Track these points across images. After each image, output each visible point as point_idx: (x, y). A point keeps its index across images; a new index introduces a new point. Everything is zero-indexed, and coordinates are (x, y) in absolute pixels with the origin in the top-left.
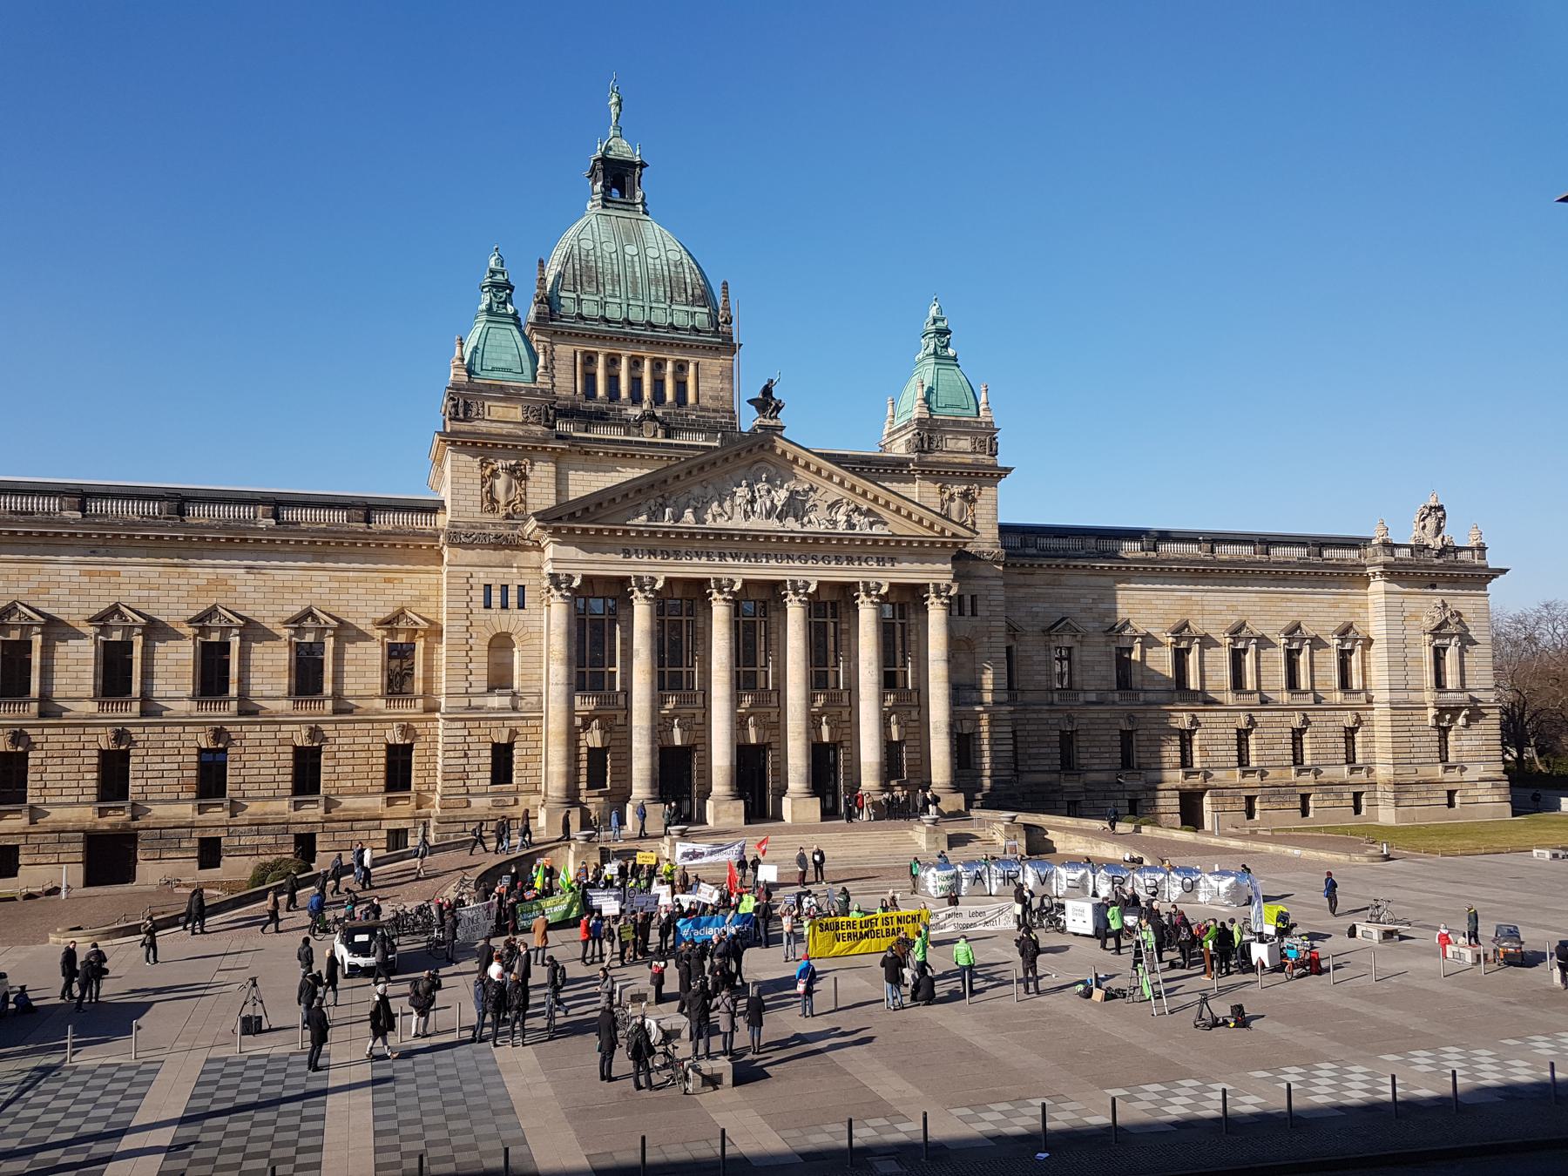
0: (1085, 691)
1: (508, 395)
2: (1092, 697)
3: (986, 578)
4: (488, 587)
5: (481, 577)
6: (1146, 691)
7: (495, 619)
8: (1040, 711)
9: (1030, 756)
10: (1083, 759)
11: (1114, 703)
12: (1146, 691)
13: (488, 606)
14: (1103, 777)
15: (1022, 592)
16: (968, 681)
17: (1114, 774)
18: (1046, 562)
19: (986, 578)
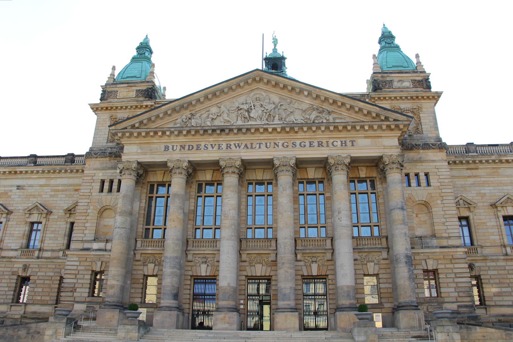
3: (434, 161)
4: (103, 182)
5: (100, 175)
8: (498, 260)
15: (471, 181)
18: (484, 159)
19: (434, 161)
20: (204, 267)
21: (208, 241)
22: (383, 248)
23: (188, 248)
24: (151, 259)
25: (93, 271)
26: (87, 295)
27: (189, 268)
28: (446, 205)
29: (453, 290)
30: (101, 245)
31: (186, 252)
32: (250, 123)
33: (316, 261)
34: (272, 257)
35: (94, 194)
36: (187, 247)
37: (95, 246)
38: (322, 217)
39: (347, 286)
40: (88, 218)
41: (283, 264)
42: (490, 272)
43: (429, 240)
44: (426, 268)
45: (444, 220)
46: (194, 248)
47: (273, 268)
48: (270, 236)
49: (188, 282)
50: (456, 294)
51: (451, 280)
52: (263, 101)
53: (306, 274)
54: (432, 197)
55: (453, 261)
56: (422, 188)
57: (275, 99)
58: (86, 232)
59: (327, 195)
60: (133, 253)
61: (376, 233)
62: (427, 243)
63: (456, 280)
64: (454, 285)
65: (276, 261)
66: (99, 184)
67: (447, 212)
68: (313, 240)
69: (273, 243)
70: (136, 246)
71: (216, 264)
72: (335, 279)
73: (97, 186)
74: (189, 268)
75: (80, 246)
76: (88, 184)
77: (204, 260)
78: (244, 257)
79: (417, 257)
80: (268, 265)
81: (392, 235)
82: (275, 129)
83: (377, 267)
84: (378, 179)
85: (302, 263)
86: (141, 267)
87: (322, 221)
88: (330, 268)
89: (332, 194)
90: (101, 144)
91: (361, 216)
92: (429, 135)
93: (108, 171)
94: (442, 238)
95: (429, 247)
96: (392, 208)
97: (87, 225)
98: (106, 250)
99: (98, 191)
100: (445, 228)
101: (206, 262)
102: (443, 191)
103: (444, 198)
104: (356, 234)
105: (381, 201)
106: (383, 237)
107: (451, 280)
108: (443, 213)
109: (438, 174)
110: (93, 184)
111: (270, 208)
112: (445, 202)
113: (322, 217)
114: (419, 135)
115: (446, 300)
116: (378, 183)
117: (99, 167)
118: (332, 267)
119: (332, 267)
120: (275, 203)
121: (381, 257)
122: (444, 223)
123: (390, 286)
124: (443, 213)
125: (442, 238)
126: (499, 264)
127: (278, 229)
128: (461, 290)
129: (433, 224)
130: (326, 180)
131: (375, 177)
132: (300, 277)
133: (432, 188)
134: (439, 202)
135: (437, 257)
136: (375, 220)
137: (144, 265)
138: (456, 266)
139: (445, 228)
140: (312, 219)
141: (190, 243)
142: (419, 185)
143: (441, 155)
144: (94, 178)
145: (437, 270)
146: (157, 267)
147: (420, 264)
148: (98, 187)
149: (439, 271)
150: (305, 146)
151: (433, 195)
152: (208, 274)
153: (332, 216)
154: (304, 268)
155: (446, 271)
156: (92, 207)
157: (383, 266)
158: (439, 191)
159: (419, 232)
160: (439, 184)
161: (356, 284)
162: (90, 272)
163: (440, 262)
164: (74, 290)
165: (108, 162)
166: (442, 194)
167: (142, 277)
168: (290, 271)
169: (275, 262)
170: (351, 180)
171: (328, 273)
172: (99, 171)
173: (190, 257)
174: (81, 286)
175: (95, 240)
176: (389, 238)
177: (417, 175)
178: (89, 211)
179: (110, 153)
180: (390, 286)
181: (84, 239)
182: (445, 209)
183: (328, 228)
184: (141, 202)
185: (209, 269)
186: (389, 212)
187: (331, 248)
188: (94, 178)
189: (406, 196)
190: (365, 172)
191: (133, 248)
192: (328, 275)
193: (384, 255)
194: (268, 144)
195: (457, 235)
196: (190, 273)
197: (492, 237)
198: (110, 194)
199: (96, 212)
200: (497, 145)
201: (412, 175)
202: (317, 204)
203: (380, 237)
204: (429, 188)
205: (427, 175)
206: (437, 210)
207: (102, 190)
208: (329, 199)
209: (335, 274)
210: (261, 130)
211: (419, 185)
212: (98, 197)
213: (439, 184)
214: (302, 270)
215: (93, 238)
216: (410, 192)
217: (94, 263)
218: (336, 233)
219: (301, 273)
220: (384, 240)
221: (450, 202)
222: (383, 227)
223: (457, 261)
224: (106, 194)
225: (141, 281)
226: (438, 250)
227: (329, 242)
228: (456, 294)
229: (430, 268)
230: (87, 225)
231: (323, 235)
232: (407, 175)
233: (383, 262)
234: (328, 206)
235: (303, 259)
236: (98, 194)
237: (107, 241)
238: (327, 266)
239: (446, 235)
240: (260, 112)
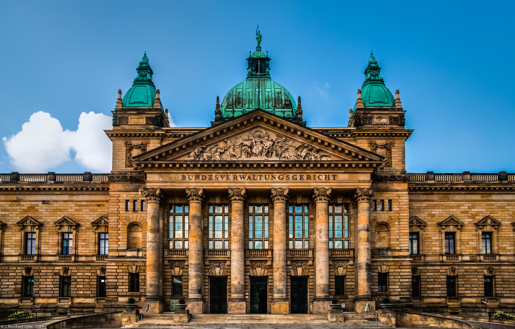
0: (462, 255)
1: (140, 112)
2: (467, 258)
3: (397, 191)
5: (124, 196)
6: (500, 255)
7: (130, 216)
9: (429, 289)
10: (461, 290)
11: (480, 261)
12: (500, 255)
13: (127, 210)
14: (473, 300)
16: (386, 246)
17: (479, 300)
19: (397, 191)
20: (217, 270)
21: (220, 251)
22: (351, 257)
23: (205, 256)
24: (177, 264)
25: (129, 273)
26: (127, 290)
27: (207, 270)
28: (401, 226)
29: (398, 287)
30: (135, 253)
31: (204, 259)
32: (253, 158)
33: (301, 266)
34: (269, 263)
35: (121, 212)
36: (204, 255)
37: (129, 254)
38: (306, 233)
39: (323, 285)
40: (119, 232)
41: (278, 268)
43: (385, 252)
44: (380, 271)
45: (398, 237)
46: (210, 256)
47: (270, 270)
48: (267, 247)
49: (207, 281)
50: (400, 290)
51: (397, 280)
52: (263, 138)
53: (293, 274)
54: (391, 219)
55: (401, 267)
56: (385, 212)
57: (273, 137)
58: (119, 243)
59: (312, 216)
60: (161, 259)
61: (346, 247)
62: (384, 254)
63: (401, 280)
64: (399, 284)
65: (272, 265)
66: (125, 204)
67: (401, 231)
68: (300, 250)
69: (270, 253)
70: (163, 254)
71: (228, 267)
72: (315, 278)
73: (123, 205)
74: (207, 270)
75: (116, 254)
76: (114, 204)
77: (217, 264)
78: (248, 263)
79: (375, 264)
80: (265, 268)
81: (358, 250)
82: (273, 165)
83: (345, 271)
84: (351, 205)
85: (291, 267)
86: (170, 270)
87: (306, 235)
88: (311, 270)
89: (315, 216)
90: (121, 168)
91: (336, 232)
92: (397, 168)
93: (131, 193)
94: (395, 250)
95: (384, 257)
96: (360, 229)
97: (119, 237)
98: (138, 257)
99: (125, 209)
100: (398, 243)
101: (219, 266)
102: (401, 214)
104: (331, 246)
105: (352, 222)
106: (352, 249)
107: (397, 280)
108: (398, 231)
109: (399, 201)
110: (119, 204)
111: (266, 225)
112: (401, 223)
113: (306, 233)
114: (388, 168)
115: (392, 294)
116: (351, 208)
117: (122, 189)
118: (313, 270)
119: (313, 270)
120: (271, 222)
121: (348, 264)
122: (398, 240)
123: (354, 283)
124: (398, 231)
125: (395, 250)
127: (275, 243)
128: (403, 287)
129: (390, 240)
130: (310, 205)
131: (349, 204)
132: (289, 277)
133: (393, 212)
134: (397, 223)
135: (390, 264)
136: (346, 235)
137: (171, 269)
138: (402, 270)
139: (398, 243)
140: (299, 234)
141: (207, 252)
142: (383, 210)
143: (405, 186)
144: (120, 198)
145: (388, 273)
146: (181, 271)
147: (377, 269)
148: (125, 207)
149: (390, 274)
150: (296, 179)
151: (393, 218)
152: (221, 275)
153: (315, 233)
154: (292, 271)
155: (395, 274)
156: (121, 223)
157: (349, 270)
158: (398, 215)
159: (378, 245)
160: (398, 209)
161: (329, 282)
162: (128, 274)
164: (116, 287)
165: (129, 184)
166: (400, 217)
167: (170, 277)
168: (283, 273)
169: (271, 267)
170: (329, 204)
171: (309, 274)
172: (122, 193)
173: (207, 263)
174: (121, 284)
175: (127, 249)
176: (356, 250)
177: (383, 201)
178: (119, 226)
179: (131, 177)
180: (354, 283)
181: (119, 248)
182: (400, 228)
183: (311, 242)
184: (164, 220)
185: (222, 271)
186: (357, 231)
187: (312, 256)
188: (120, 198)
189: (372, 218)
190: (341, 199)
191: (161, 256)
192: (309, 276)
193: (351, 262)
194: (267, 176)
195: (407, 248)
196: (208, 274)
198: (135, 212)
199: (125, 227)
200: (452, 174)
202: (303, 223)
203: (349, 250)
204: (391, 212)
205: (390, 201)
206: (394, 230)
207: (127, 210)
208: (312, 220)
209: (315, 275)
210: (262, 166)
212: (125, 215)
213: (398, 209)
214: (290, 272)
215: (126, 248)
216: (375, 215)
217: (130, 268)
218: (317, 247)
219: (289, 274)
220: (352, 252)
221: (405, 223)
222: (352, 242)
224: (132, 212)
225: (170, 280)
226: (391, 259)
227: (311, 252)
228: (400, 290)
229: (384, 271)
230: (119, 237)
231: (306, 247)
232: (375, 201)
233: (349, 267)
234: (312, 225)
235: (291, 264)
236: (125, 212)
237: (138, 251)
238: (309, 269)
239: (399, 248)
240: (260, 148)
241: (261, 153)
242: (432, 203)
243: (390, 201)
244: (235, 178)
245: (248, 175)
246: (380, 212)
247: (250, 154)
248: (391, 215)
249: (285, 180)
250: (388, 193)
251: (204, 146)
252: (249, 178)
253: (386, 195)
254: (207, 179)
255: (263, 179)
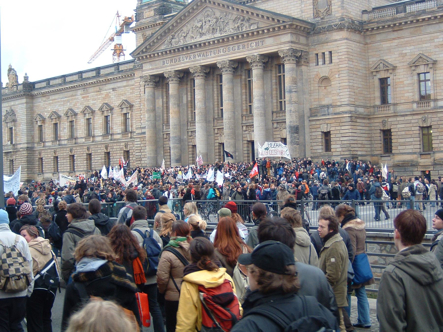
42: (399, 126)
62: (325, 111)
85: (247, 132)
103: (341, 72)
126: (407, 118)
133: (333, 64)
142: (324, 63)
151: (333, 70)
158: (337, 67)
163: (332, 125)
177: (324, 53)
197: (406, 95)
201: (320, 55)
205: (331, 52)
211: (324, 63)
223: (343, 124)
241: (208, 31)
242: (403, 40)
243: (331, 52)
244: (194, 57)
245: (202, 53)
246: (322, 66)
247: (202, 34)
248: (331, 68)
249: (227, 52)
250: (328, 44)
251: (173, 34)
252: (203, 55)
253: (327, 47)
254: (178, 61)
255: (212, 54)
